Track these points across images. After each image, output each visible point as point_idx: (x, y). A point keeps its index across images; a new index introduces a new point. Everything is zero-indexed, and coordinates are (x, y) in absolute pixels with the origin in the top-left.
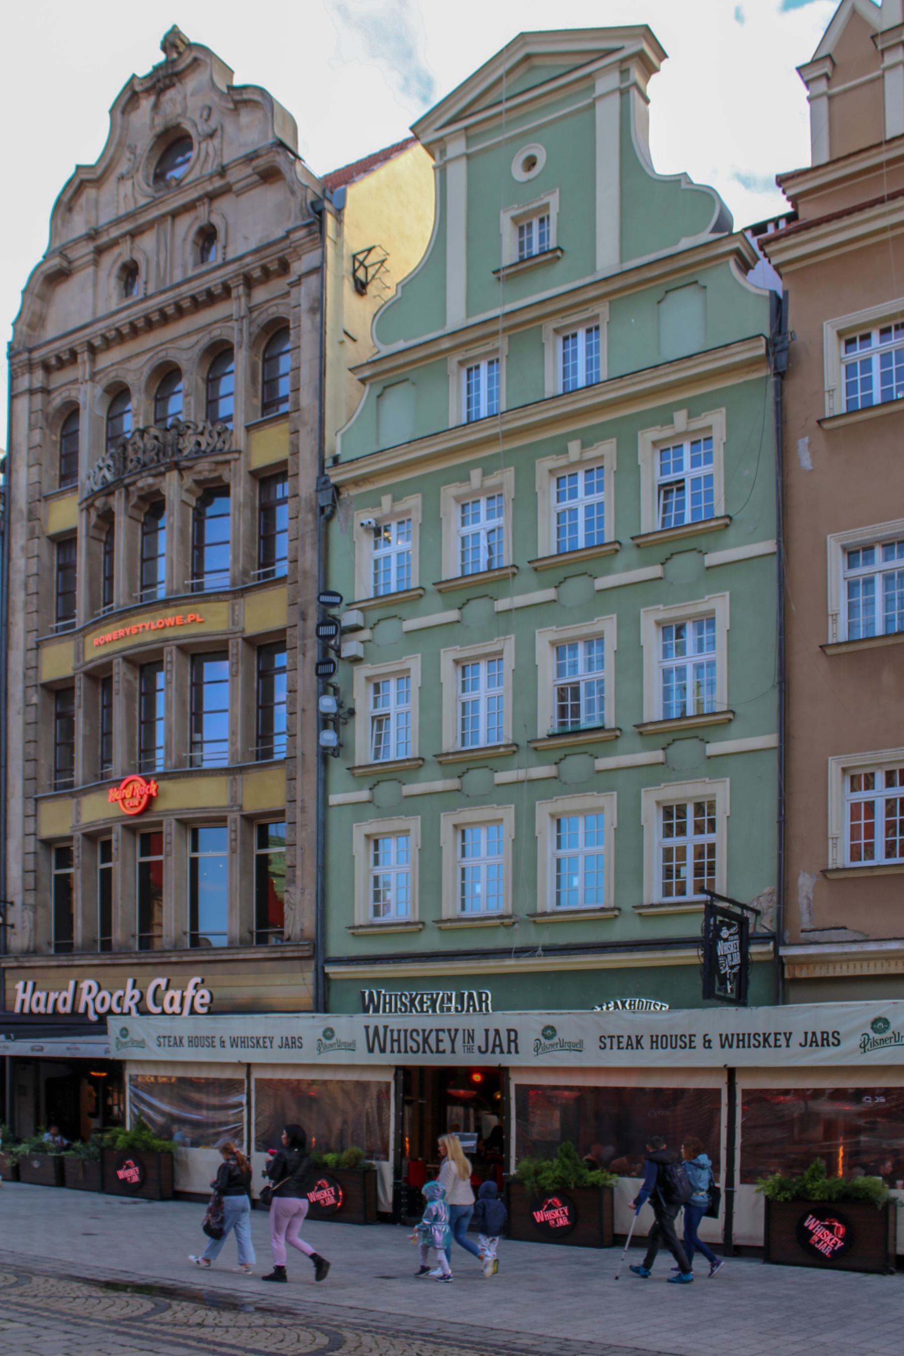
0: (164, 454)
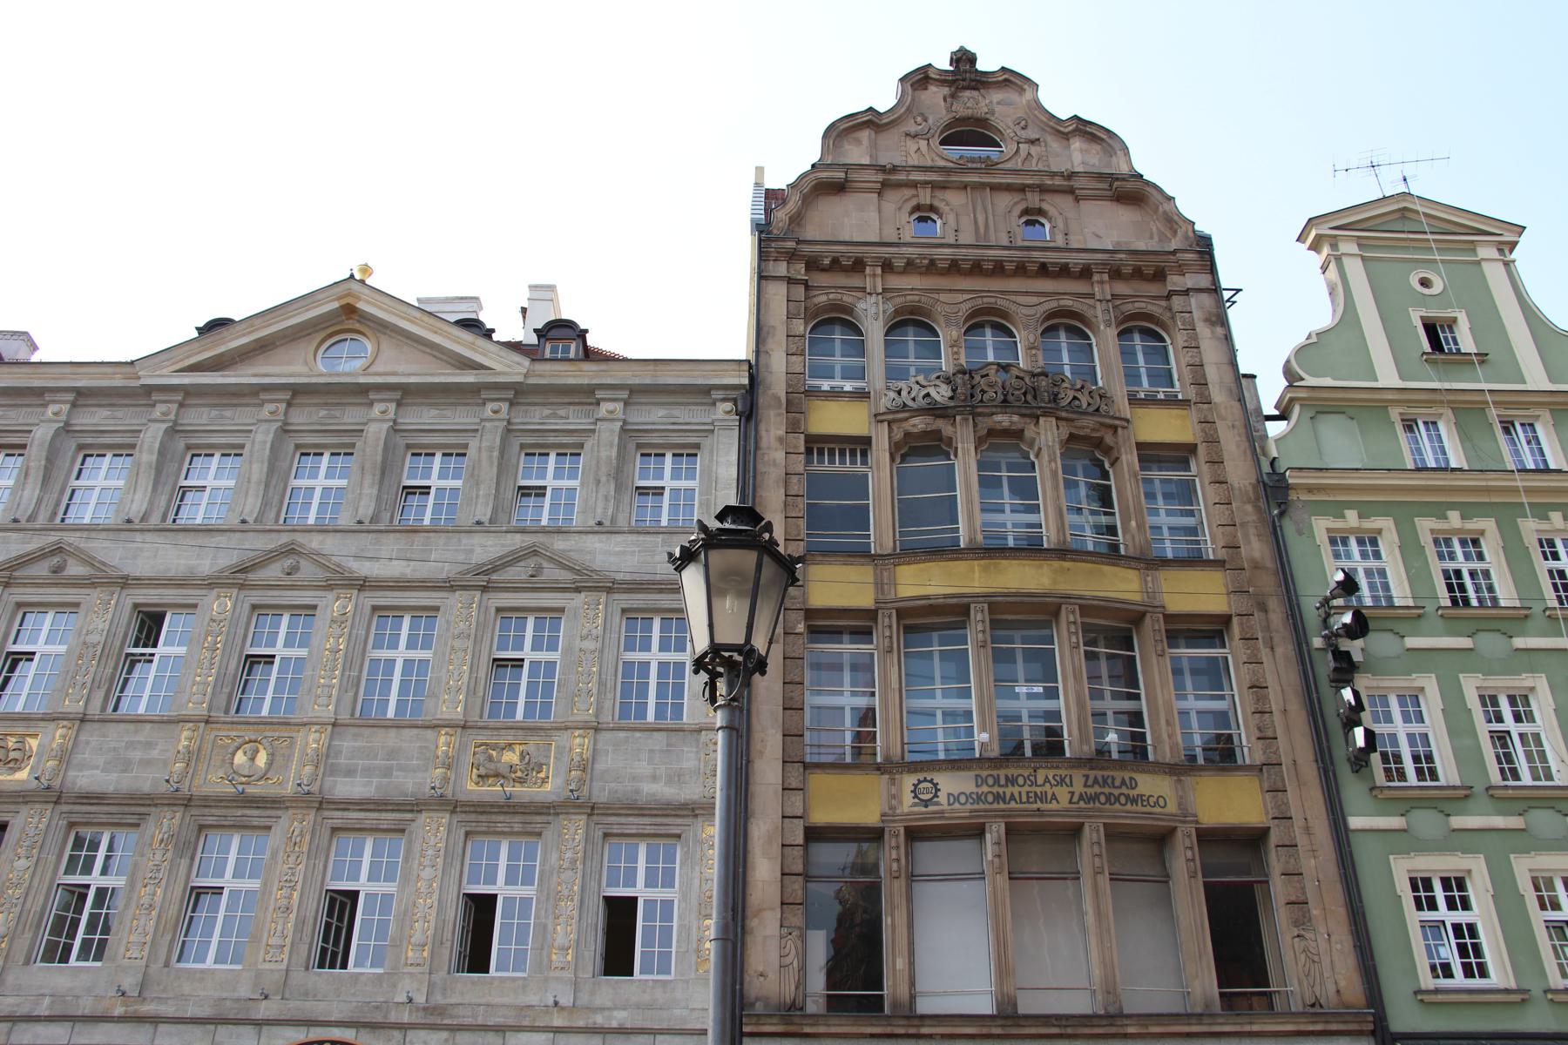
0: (1035, 397)
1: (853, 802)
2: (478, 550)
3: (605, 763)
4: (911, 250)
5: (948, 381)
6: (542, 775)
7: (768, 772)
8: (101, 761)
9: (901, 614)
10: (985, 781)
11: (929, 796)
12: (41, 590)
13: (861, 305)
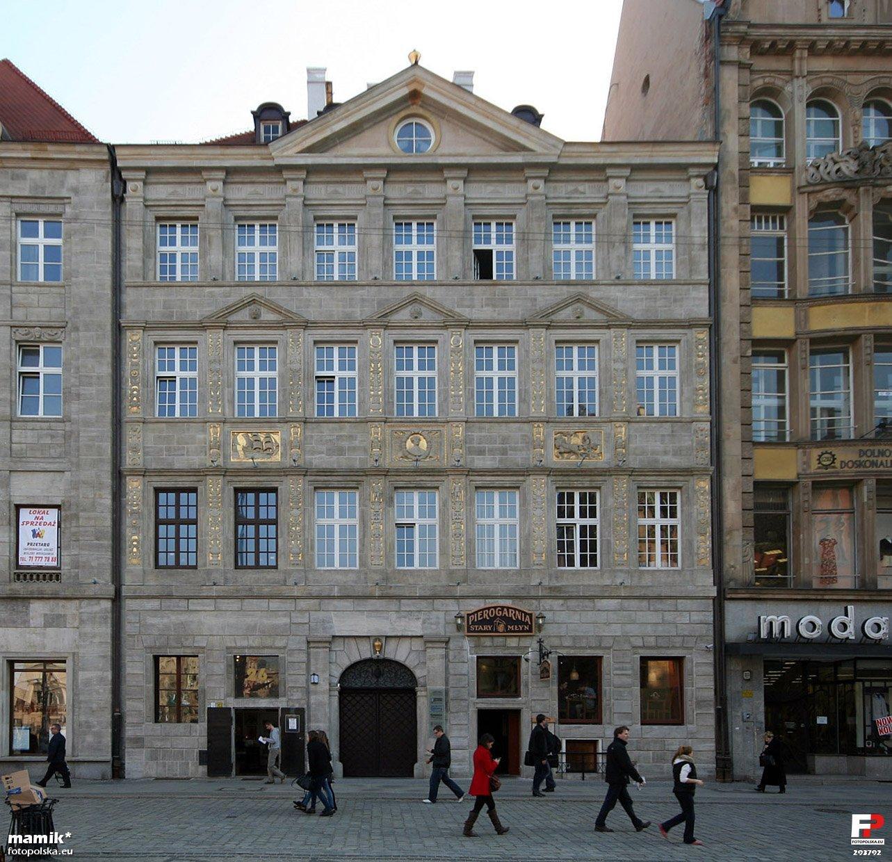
1: (781, 466)
2: (539, 299)
3: (636, 444)
4: (833, 32)
5: (857, 158)
6: (598, 451)
7: (733, 448)
8: (324, 448)
9: (813, 341)
10: (865, 453)
11: (828, 463)
12: (249, 332)
13: (788, 88)
